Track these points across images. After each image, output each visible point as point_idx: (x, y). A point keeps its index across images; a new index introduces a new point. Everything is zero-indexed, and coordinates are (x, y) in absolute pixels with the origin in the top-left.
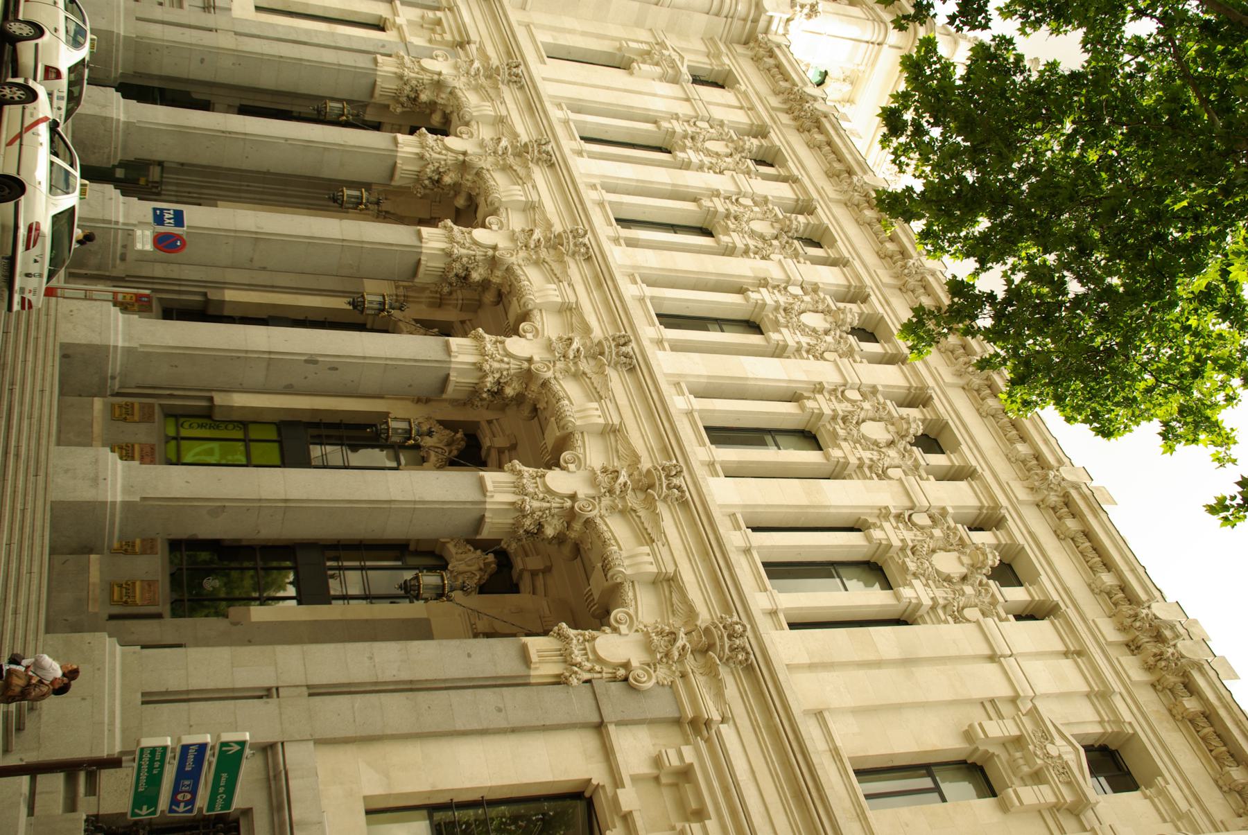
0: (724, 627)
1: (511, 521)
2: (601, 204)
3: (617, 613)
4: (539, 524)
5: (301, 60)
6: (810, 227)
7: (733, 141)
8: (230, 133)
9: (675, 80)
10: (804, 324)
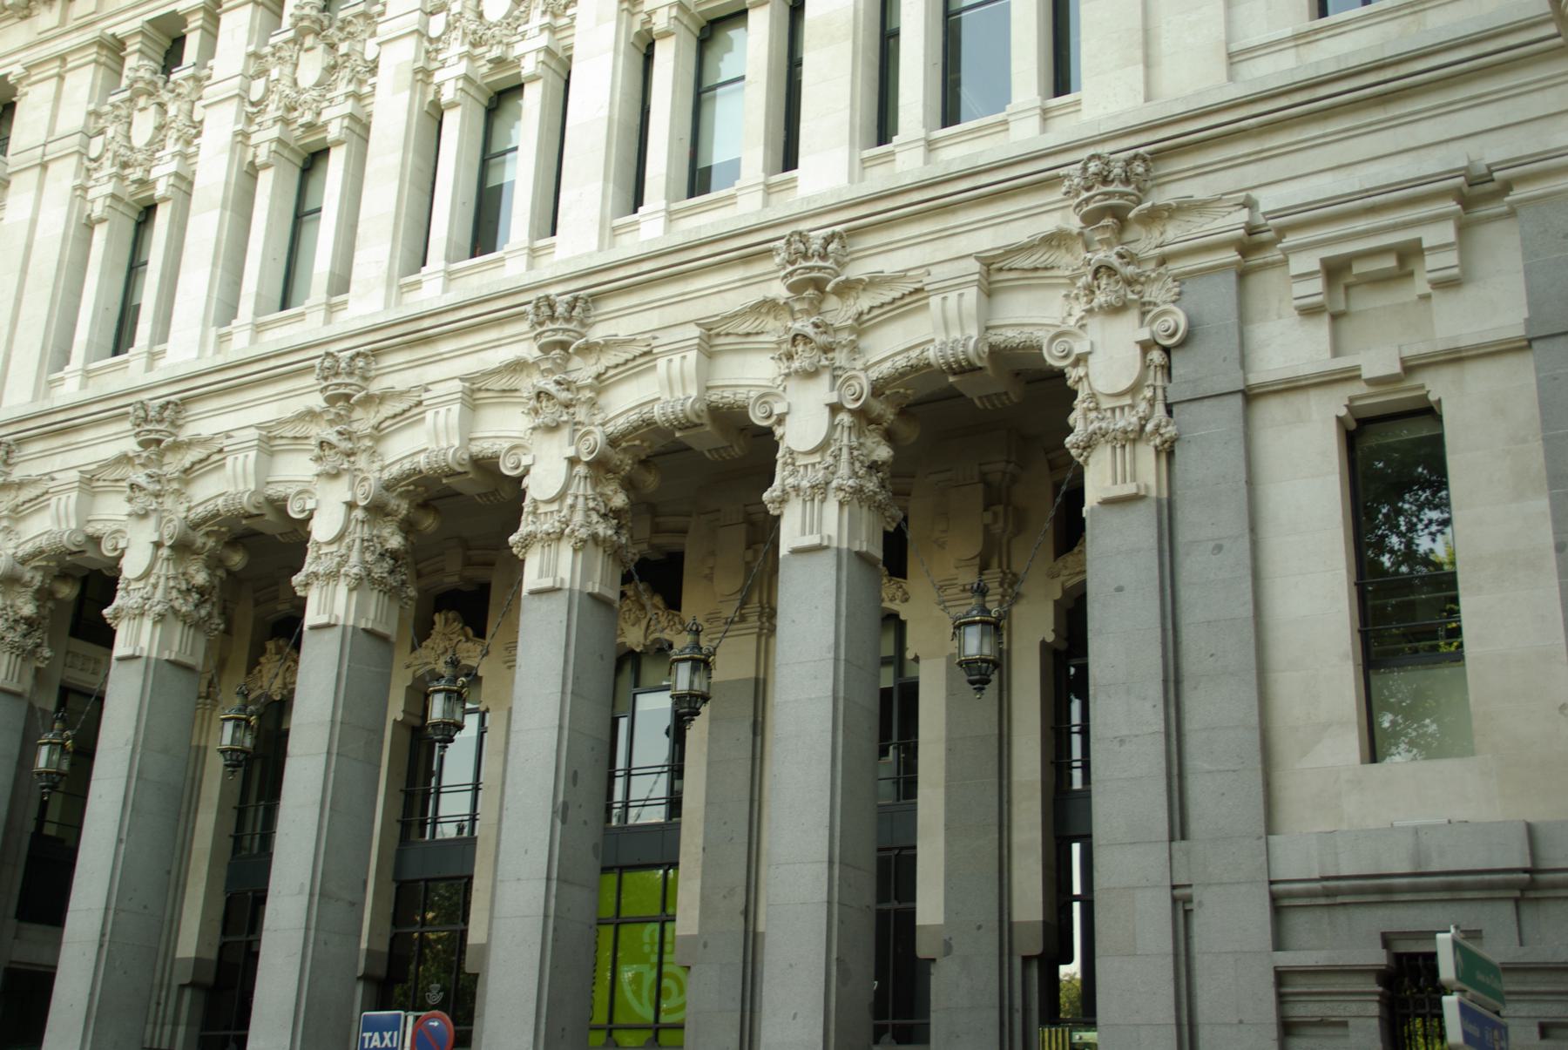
0: (1088, 189)
1: (865, 509)
2: (258, 328)
3: (757, 417)
4: (870, 467)
6: (145, 49)
7: (131, 100)
8: (103, 935)
10: (506, 17)
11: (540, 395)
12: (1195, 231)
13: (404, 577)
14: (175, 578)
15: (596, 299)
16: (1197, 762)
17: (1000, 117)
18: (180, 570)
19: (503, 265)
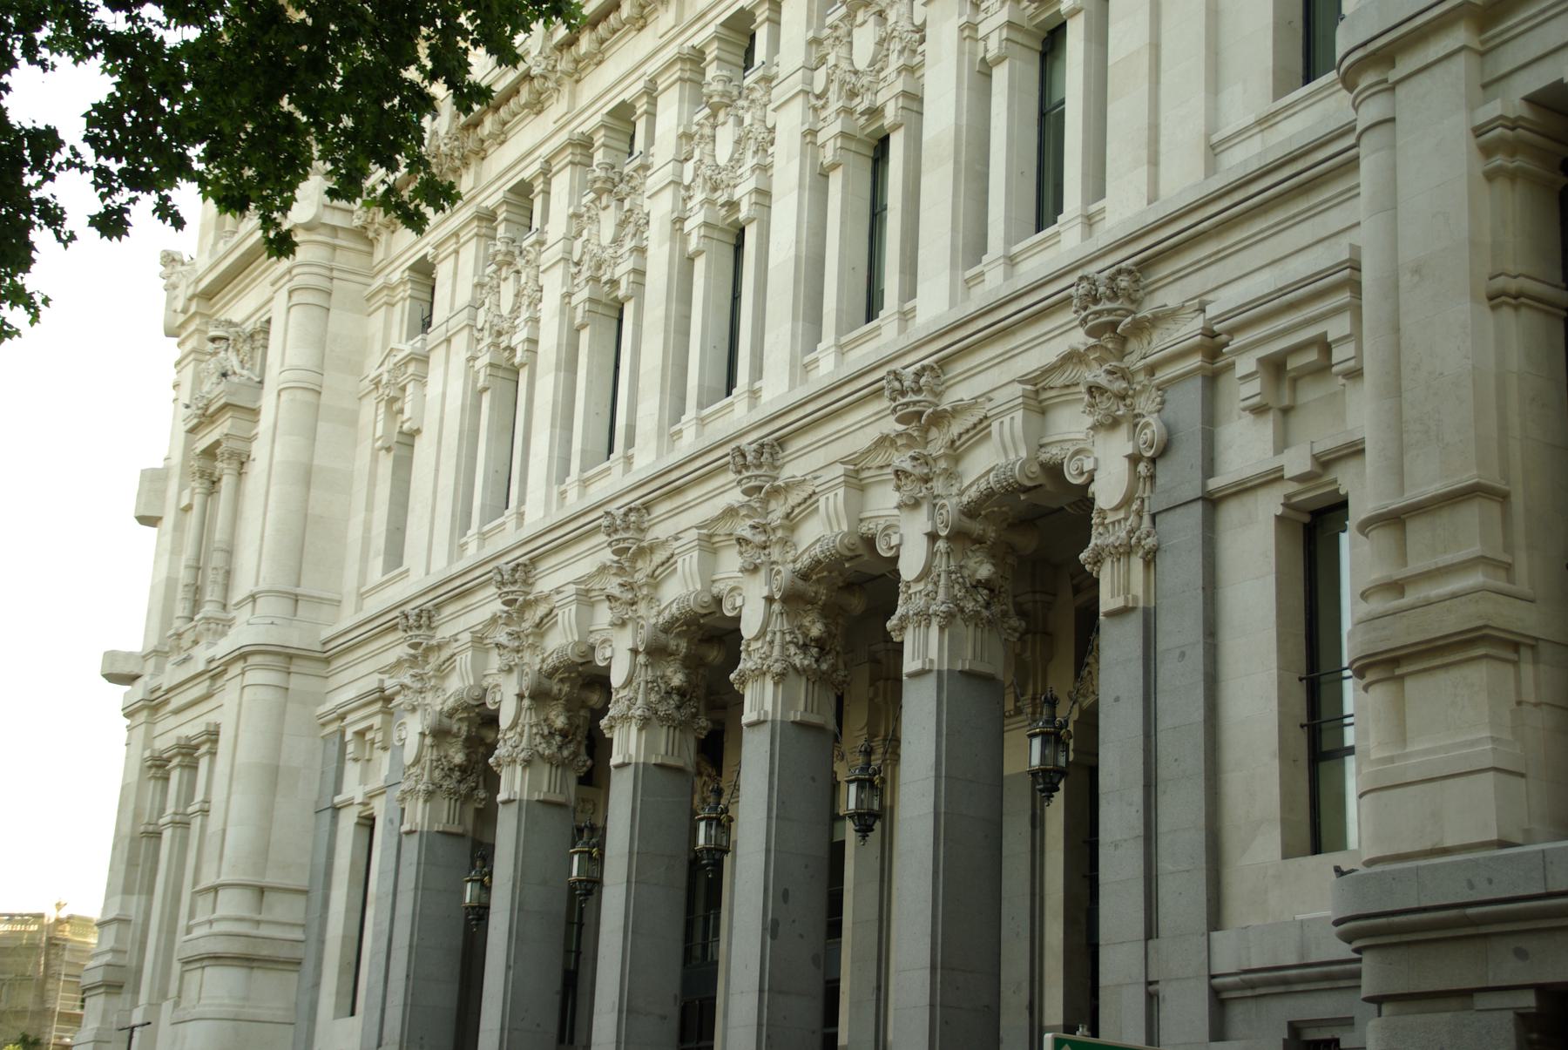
0: (1085, 309)
5: (411, 946)
9: (423, 359)
10: (731, 160)
11: (1093, 390)
12: (1167, 340)
13: (1004, 607)
14: (537, 725)
15: (781, 443)
17: (401, 569)
18: (542, 717)
19: (880, 334)
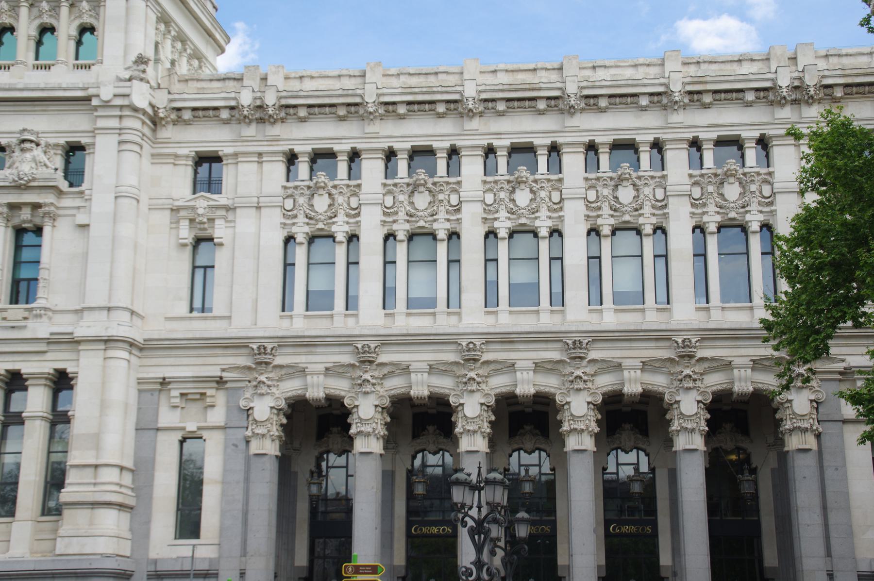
16: (833, 534)
